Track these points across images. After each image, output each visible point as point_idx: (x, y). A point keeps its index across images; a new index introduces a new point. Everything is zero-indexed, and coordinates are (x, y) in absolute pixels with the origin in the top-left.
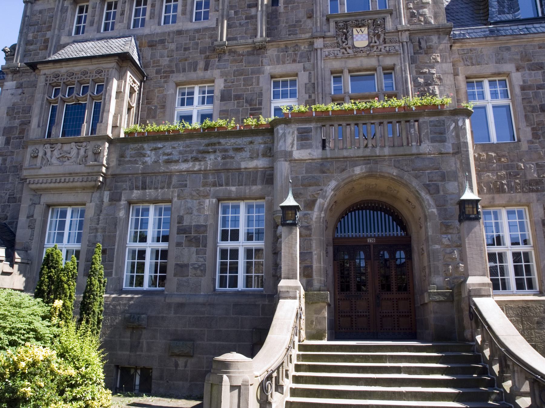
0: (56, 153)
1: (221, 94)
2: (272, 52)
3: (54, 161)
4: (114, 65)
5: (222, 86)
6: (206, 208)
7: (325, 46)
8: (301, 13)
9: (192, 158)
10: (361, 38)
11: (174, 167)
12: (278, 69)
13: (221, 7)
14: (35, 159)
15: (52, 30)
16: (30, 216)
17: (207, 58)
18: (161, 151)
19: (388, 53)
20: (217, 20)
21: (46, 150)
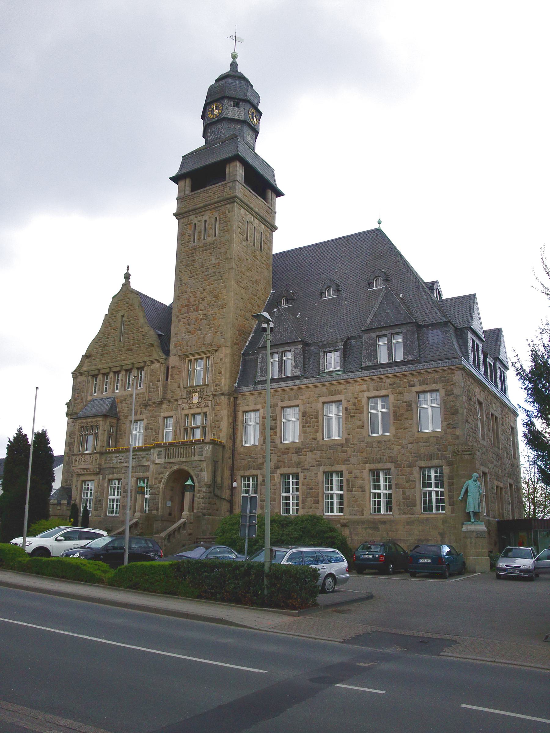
2: (164, 406)
7: (183, 403)
8: (176, 385)
10: (195, 399)
16: (76, 486)
17: (141, 408)
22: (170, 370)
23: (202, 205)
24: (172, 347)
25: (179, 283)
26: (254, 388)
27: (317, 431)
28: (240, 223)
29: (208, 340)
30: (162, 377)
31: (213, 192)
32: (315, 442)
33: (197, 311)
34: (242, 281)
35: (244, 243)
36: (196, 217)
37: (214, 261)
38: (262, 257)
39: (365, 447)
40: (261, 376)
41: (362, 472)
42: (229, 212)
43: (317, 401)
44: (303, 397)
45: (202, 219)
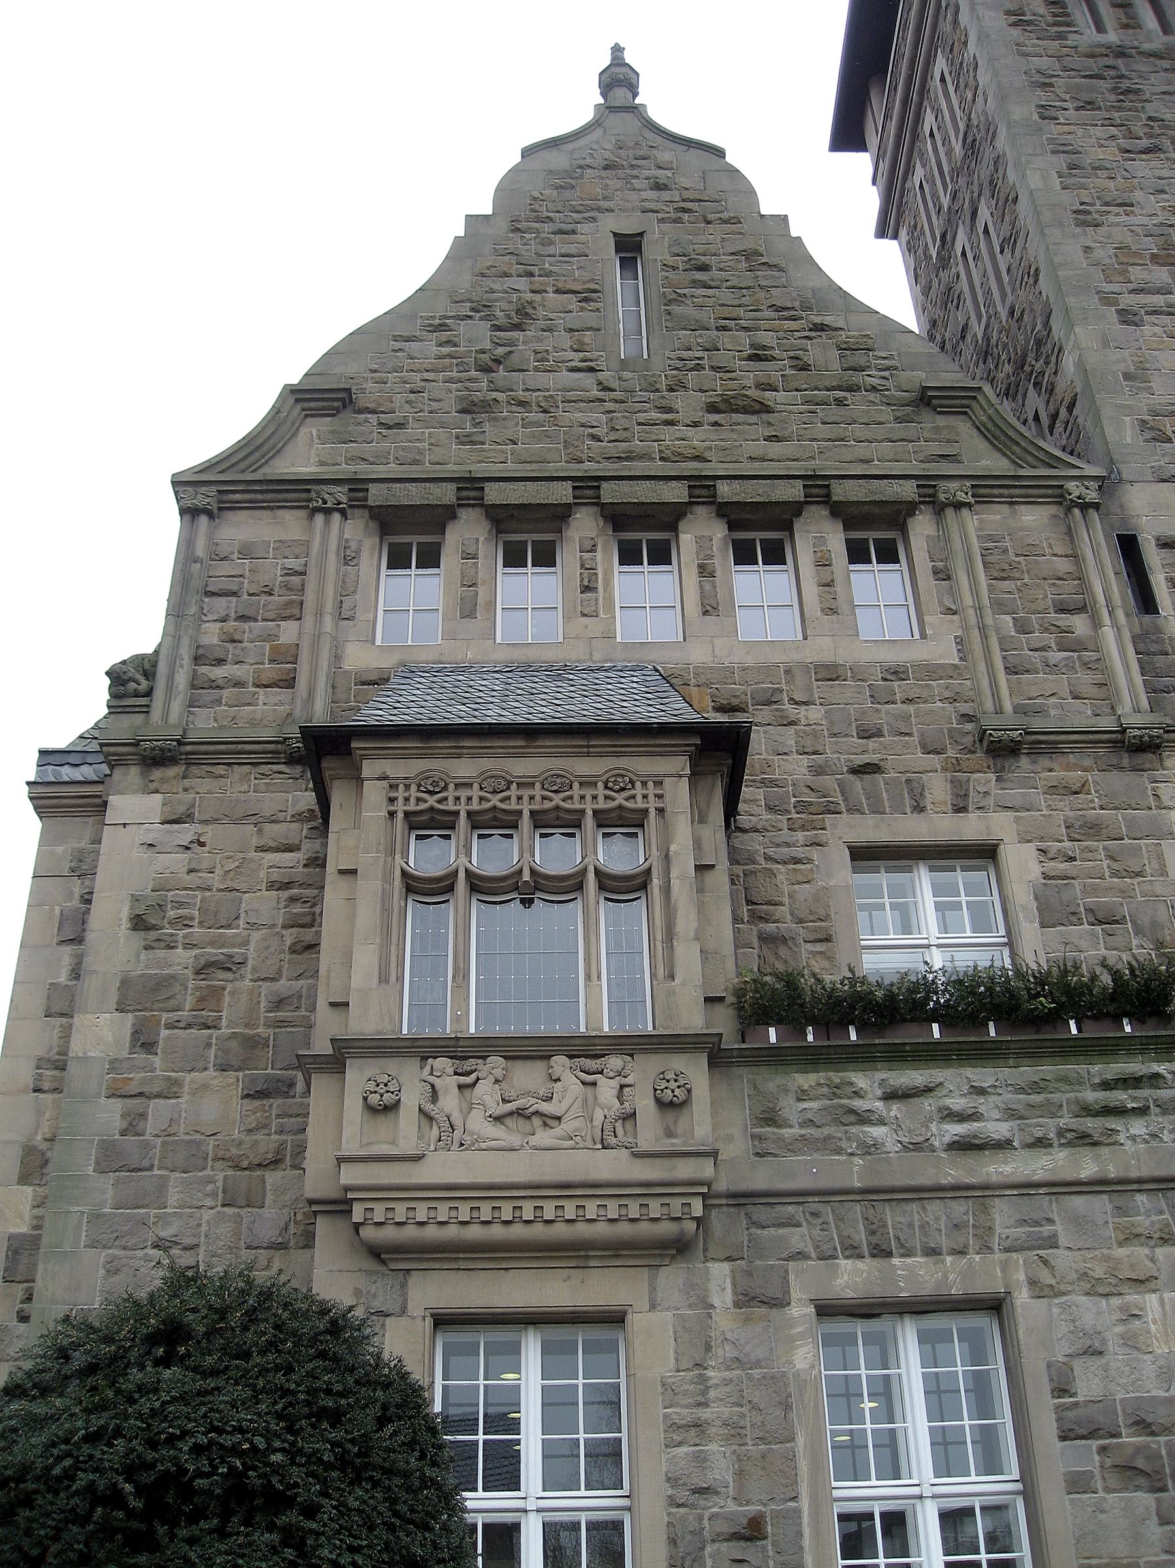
0: (486, 1092)
1: (1036, 898)
3: (478, 1123)
4: (681, 764)
5: (1035, 870)
6: (1153, 1328)
9: (1061, 1133)
13: (968, 601)
14: (391, 1115)
15: (309, 619)
18: (927, 1104)
20: (959, 641)
21: (438, 1082)
22: (1153, 557)
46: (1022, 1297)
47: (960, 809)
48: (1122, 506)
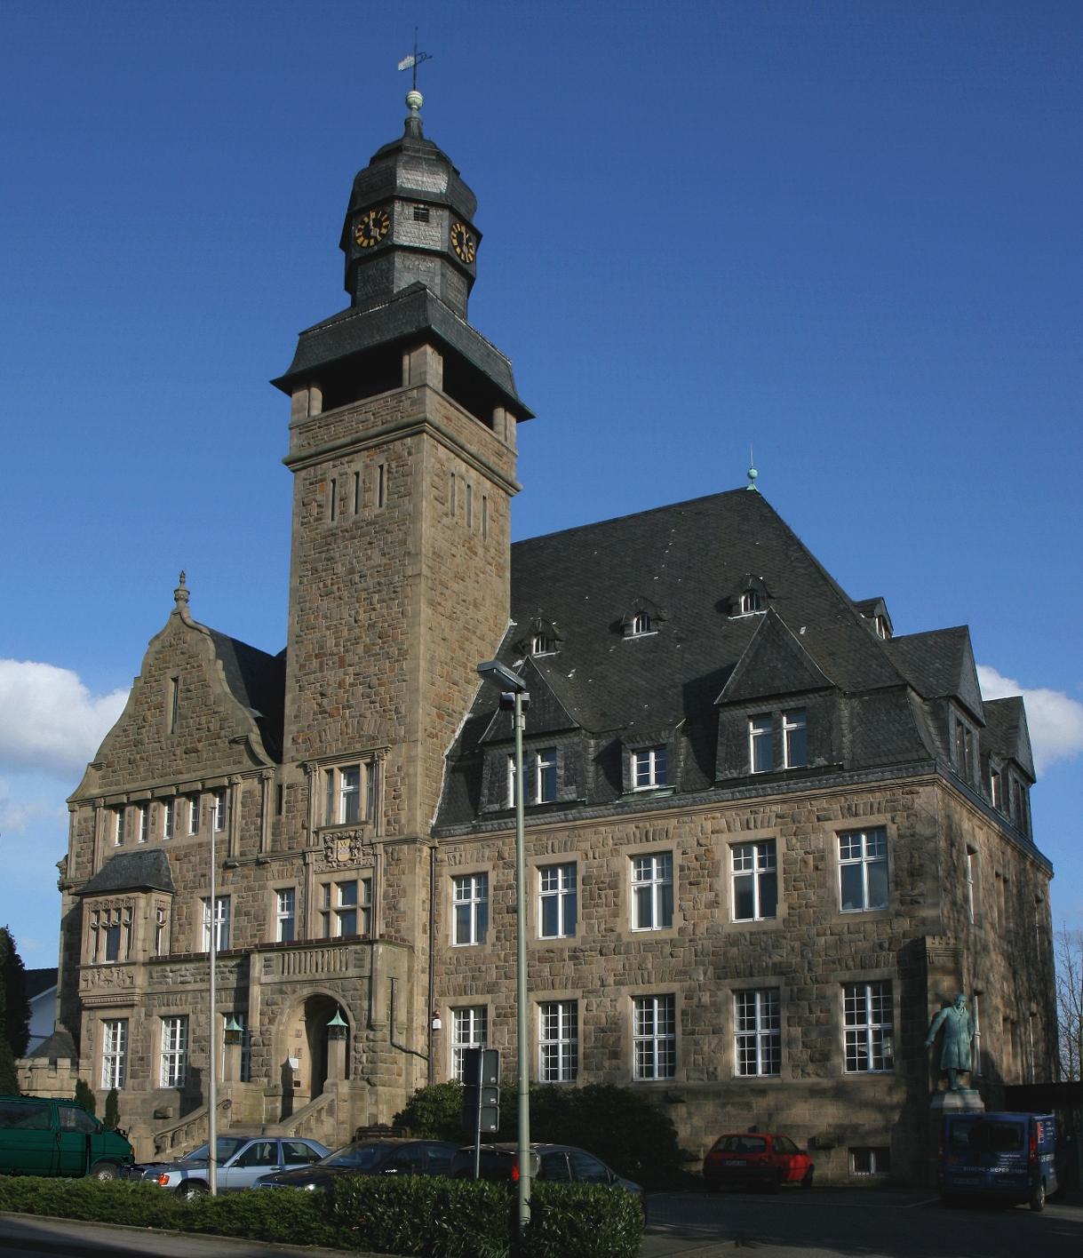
10: (342, 852)
11: (189, 987)
12: (281, 884)
18: (178, 973)
19: (365, 867)
22: (285, 792)
23: (348, 439)
24: (287, 743)
25: (298, 607)
26: (474, 827)
27: (616, 915)
28: (435, 478)
29: (369, 728)
30: (270, 807)
31: (373, 411)
32: (613, 936)
33: (340, 667)
34: (443, 603)
35: (445, 520)
36: (334, 466)
37: (377, 559)
38: (486, 549)
39: (721, 944)
40: (490, 802)
41: (716, 996)
42: (410, 454)
43: (615, 852)
44: (586, 846)
45: (349, 471)
46: (191, 1014)
47: (222, 885)
48: (281, 774)
